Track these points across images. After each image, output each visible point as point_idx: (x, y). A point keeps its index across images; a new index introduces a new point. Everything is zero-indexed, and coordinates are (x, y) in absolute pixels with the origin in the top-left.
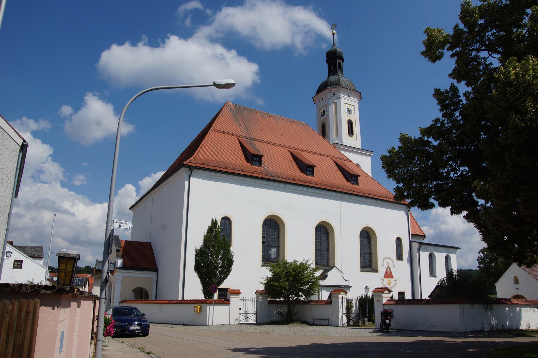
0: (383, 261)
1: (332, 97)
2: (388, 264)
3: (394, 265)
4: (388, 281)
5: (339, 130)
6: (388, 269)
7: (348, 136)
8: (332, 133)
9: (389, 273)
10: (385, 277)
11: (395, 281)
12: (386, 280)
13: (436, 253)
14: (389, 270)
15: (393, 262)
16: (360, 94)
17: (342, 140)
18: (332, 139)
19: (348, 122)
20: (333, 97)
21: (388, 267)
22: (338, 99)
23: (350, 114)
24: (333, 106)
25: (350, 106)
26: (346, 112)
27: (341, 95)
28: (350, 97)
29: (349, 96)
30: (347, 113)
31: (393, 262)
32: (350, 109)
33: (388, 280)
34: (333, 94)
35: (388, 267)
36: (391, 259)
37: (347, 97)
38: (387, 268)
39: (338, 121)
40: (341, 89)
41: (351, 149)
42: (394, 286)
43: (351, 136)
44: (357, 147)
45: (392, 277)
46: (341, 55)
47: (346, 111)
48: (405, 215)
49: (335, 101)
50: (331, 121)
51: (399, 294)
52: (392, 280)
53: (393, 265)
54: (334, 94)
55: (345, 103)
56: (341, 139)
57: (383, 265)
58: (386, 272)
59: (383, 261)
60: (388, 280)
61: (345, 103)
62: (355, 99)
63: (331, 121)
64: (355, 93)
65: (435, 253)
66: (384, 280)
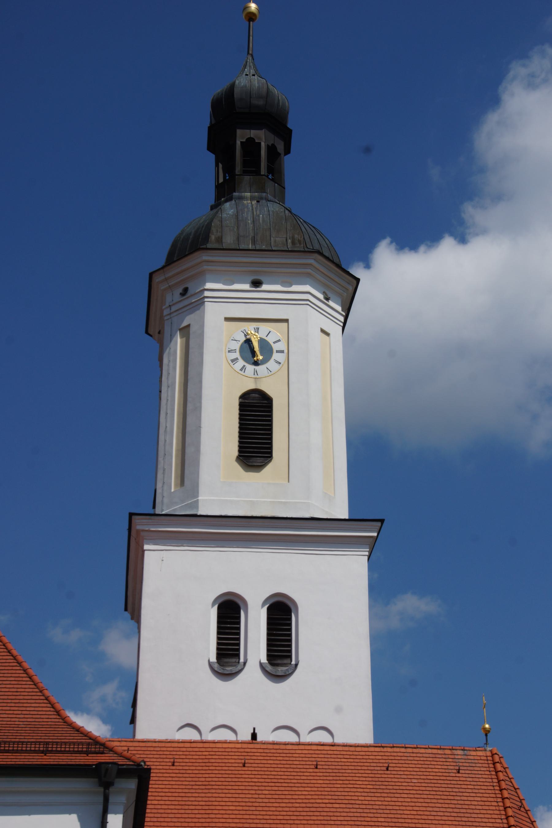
1: (174, 309)
5: (189, 450)
7: (238, 468)
8: (164, 470)
17: (198, 497)
18: (163, 497)
20: (186, 302)
22: (198, 309)
23: (256, 363)
24: (179, 341)
25: (264, 328)
26: (234, 361)
27: (209, 285)
28: (265, 287)
29: (256, 284)
30: (241, 363)
32: (263, 343)
34: (180, 290)
37: (247, 287)
39: (190, 407)
40: (205, 256)
43: (258, 467)
44: (307, 516)
46: (261, 102)
47: (237, 355)
49: (185, 324)
50: (167, 414)
54: (186, 290)
55: (227, 319)
56: (195, 492)
61: (227, 319)
62: (295, 288)
63: (167, 414)
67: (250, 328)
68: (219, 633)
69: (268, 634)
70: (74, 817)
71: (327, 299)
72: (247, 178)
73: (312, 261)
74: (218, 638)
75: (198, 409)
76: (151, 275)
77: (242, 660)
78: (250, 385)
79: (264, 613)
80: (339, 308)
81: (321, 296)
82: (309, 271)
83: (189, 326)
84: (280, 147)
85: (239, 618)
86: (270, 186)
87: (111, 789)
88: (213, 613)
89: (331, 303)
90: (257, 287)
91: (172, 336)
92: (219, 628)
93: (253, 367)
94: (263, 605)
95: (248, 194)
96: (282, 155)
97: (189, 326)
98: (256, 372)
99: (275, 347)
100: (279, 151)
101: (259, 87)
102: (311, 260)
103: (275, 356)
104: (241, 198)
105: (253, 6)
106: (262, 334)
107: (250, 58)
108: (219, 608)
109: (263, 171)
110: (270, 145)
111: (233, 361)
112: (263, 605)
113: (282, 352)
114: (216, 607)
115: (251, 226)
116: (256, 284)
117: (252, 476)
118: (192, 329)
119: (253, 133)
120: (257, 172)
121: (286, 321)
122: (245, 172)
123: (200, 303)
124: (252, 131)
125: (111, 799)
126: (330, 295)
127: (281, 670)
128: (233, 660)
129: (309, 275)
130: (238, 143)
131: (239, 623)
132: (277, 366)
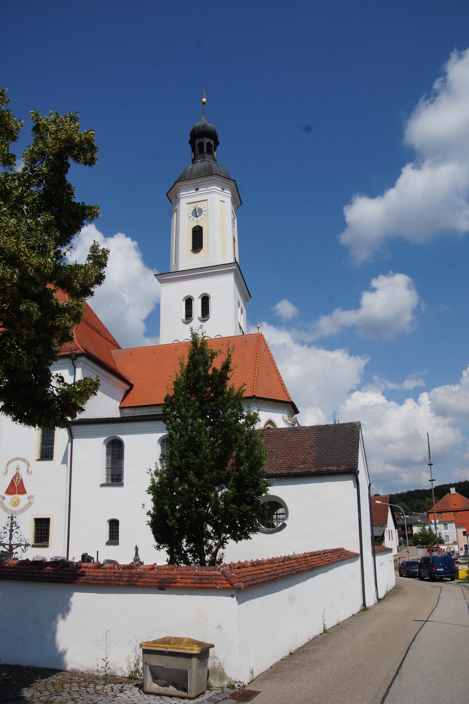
0: (8, 465)
2: (18, 469)
3: (30, 471)
4: (15, 499)
6: (17, 478)
7: (192, 253)
9: (16, 486)
10: (8, 492)
11: (29, 498)
12: (9, 498)
13: (125, 438)
14: (19, 479)
15: (28, 465)
16: (215, 175)
19: (193, 232)
21: (17, 475)
23: (197, 217)
24: (175, 214)
27: (181, 194)
28: (200, 190)
30: (192, 217)
31: (28, 465)
33: (14, 498)
34: (175, 198)
35: (17, 475)
36: (24, 460)
38: (15, 477)
41: (188, 273)
42: (26, 508)
45: (22, 491)
47: (191, 215)
48: (70, 375)
51: (36, 523)
52: (23, 499)
53: (28, 471)
55: (188, 204)
57: (7, 471)
58: (12, 483)
59: (8, 465)
60: (14, 498)
61: (188, 204)
62: (210, 188)
64: (218, 179)
65: (123, 438)
66: (5, 498)
67: (194, 205)
68: (186, 309)
69: (202, 307)
70: (67, 370)
71: (223, 189)
72: (208, 155)
73: (214, 178)
74: (186, 311)
75: (179, 236)
76: (167, 194)
77: (193, 317)
78: (195, 224)
79: (200, 301)
80: (229, 192)
81: (221, 189)
82: (214, 181)
83: (177, 209)
84: (212, 142)
85: (192, 304)
86: (208, 156)
87: (74, 361)
88: (184, 303)
89: (225, 191)
90: (197, 190)
91: (173, 213)
92: (186, 308)
93: (196, 218)
94: (199, 298)
95: (199, 161)
96: (213, 146)
97: (177, 209)
98: (197, 219)
99: (204, 210)
100: (211, 143)
101: (202, 125)
102: (214, 177)
103: (204, 213)
104: (197, 162)
105: (204, 100)
106: (199, 206)
107: (204, 116)
108: (186, 301)
109: (205, 151)
110: (208, 142)
111: (189, 217)
112: (199, 298)
113: (206, 211)
114: (184, 301)
115: (196, 170)
116: (197, 189)
117: (197, 255)
118: (178, 210)
119: (201, 140)
120: (203, 153)
121: (207, 200)
122: (200, 154)
123: (179, 200)
124: (201, 139)
125: (75, 364)
126: (224, 188)
127: (206, 319)
128: (191, 318)
129: (214, 183)
130: (196, 144)
131: (192, 305)
132: (204, 216)
